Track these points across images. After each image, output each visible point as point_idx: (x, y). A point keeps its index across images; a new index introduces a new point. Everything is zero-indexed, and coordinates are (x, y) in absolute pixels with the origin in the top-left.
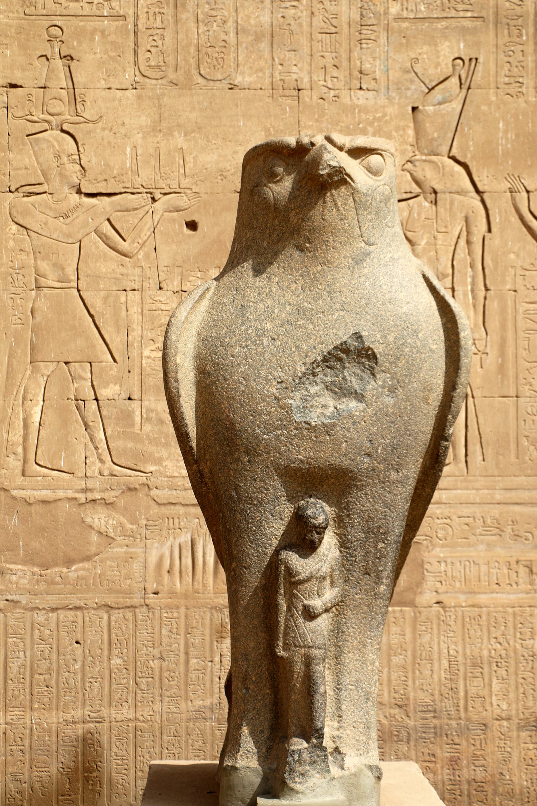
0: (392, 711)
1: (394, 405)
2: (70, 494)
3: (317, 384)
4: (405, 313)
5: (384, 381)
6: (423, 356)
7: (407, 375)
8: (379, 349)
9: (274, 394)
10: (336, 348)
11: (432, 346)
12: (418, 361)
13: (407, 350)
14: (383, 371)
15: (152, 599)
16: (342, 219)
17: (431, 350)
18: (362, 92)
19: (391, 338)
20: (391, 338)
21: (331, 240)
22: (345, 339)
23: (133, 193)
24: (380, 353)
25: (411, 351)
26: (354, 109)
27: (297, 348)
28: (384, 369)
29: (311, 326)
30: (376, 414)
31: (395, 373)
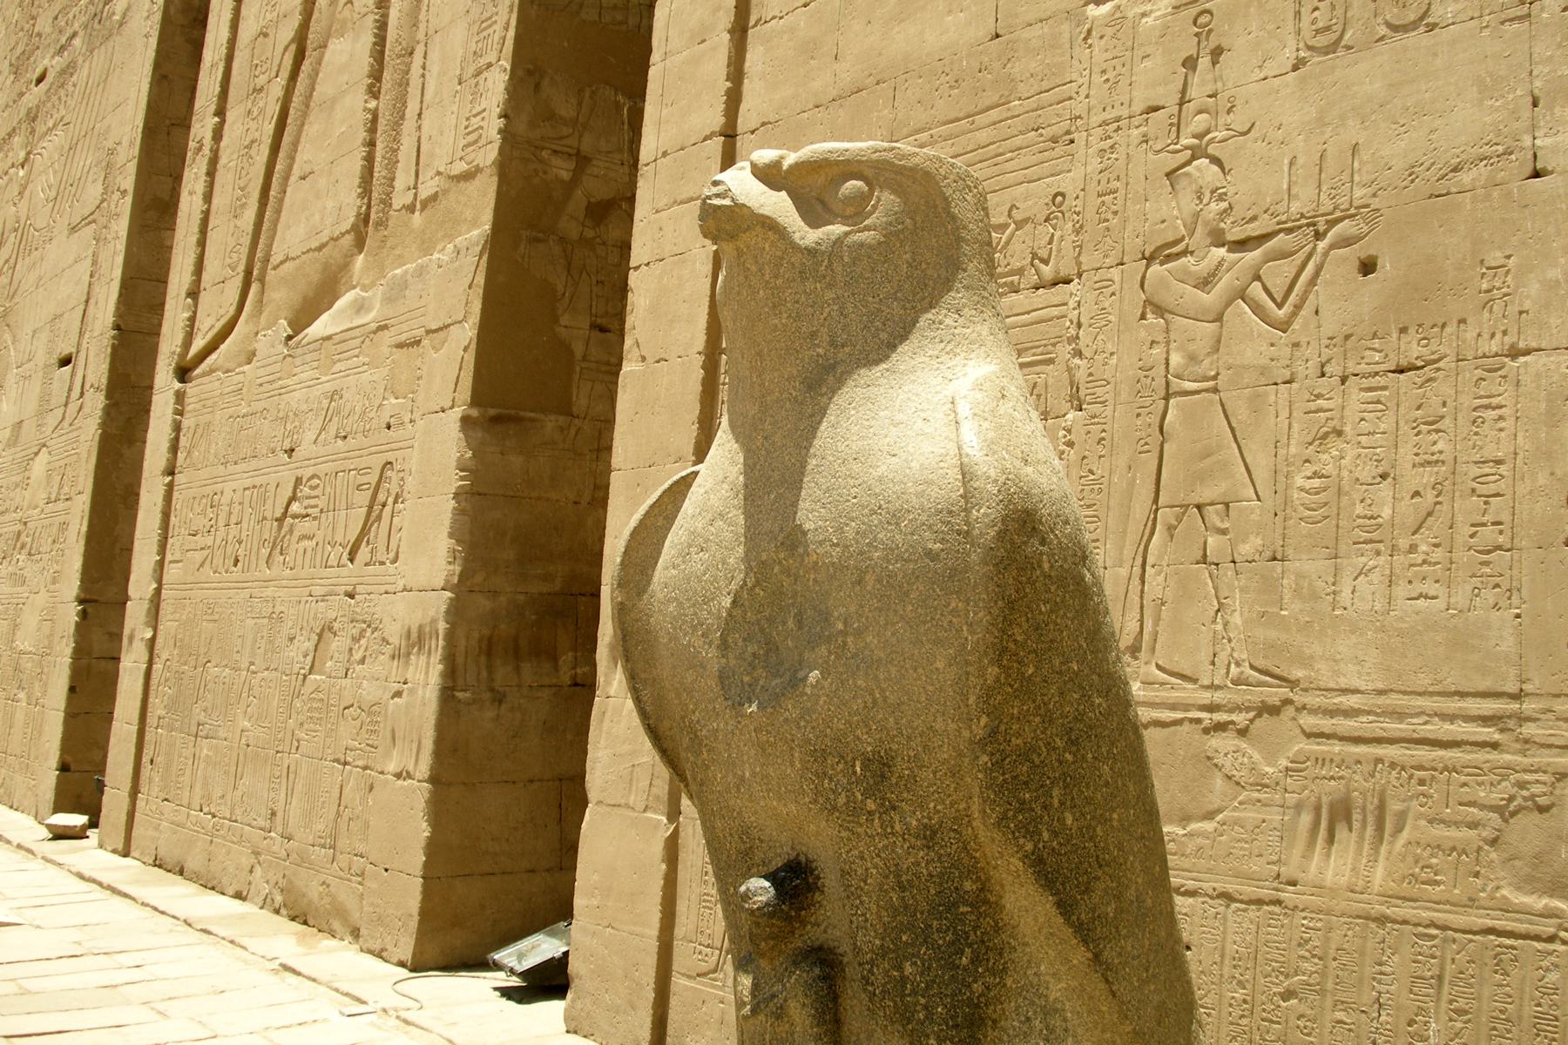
15: (1288, 895)
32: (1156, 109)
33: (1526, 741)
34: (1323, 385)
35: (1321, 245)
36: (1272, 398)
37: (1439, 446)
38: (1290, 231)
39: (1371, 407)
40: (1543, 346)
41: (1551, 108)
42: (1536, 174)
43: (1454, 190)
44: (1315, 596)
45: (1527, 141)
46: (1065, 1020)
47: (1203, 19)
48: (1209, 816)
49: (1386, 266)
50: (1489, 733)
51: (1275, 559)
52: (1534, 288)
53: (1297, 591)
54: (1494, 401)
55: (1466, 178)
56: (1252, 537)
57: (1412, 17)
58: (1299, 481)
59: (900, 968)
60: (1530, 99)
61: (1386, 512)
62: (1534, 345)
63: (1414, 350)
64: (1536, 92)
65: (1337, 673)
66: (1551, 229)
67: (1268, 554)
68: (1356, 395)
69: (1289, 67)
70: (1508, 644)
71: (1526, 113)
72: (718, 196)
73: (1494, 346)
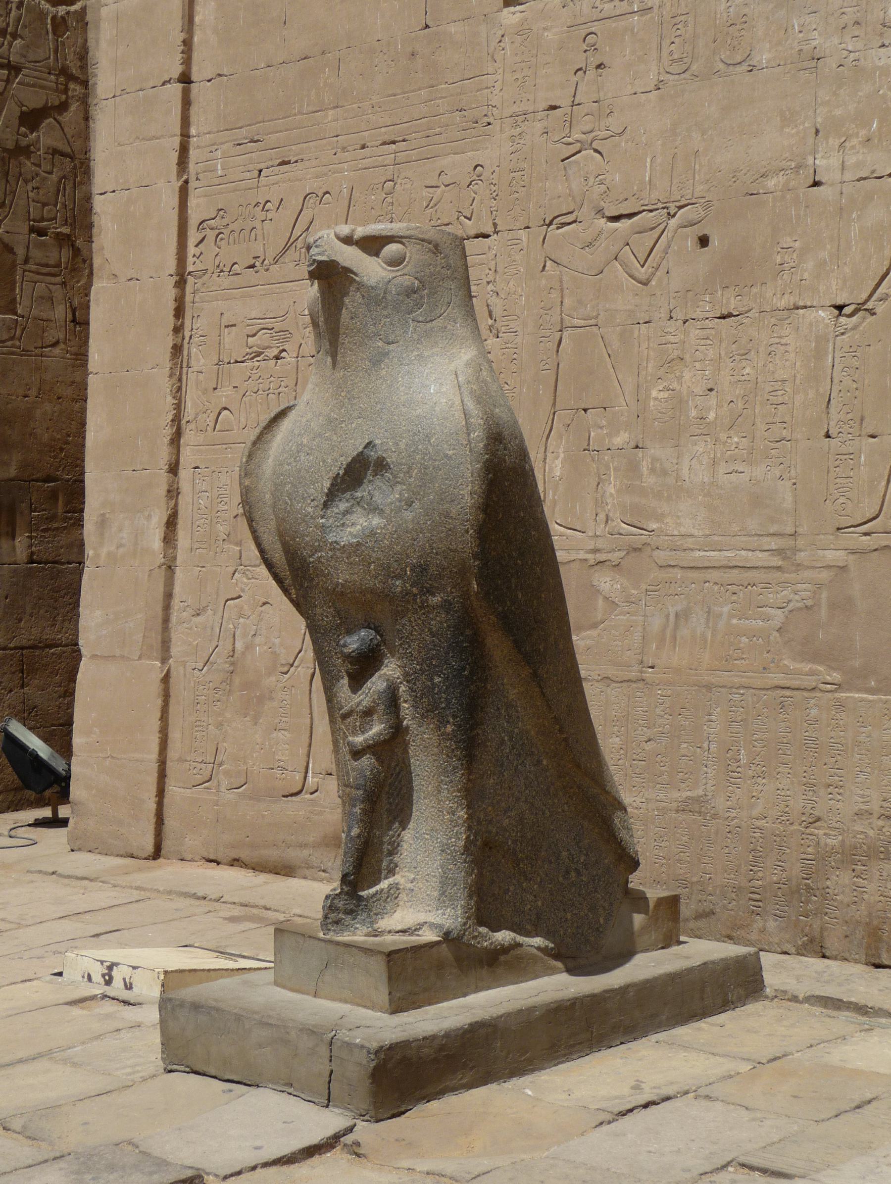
0: (881, 823)
1: (413, 521)
2: (582, 555)
4: (418, 416)
5: (400, 494)
7: (421, 486)
9: (309, 513)
17: (446, 456)
18: (883, 50)
20: (402, 446)
22: (360, 449)
24: (393, 462)
25: (423, 458)
26: (875, 73)
27: (324, 461)
29: (335, 437)
30: (396, 531)
32: (554, 108)
33: (799, 565)
34: (671, 327)
35: (673, 222)
36: (636, 333)
37: (747, 370)
38: (651, 211)
39: (703, 342)
40: (814, 304)
41: (827, 139)
42: (816, 184)
43: (761, 191)
44: (665, 473)
45: (810, 160)
46: (517, 712)
47: (591, 39)
48: (594, 626)
49: (714, 242)
50: (776, 561)
51: (637, 447)
52: (810, 265)
53: (653, 470)
54: (783, 341)
55: (771, 183)
56: (622, 433)
57: (739, 58)
58: (654, 393)
59: (432, 680)
60: (814, 131)
61: (712, 416)
62: (809, 304)
63: (733, 305)
64: (818, 126)
65: (679, 525)
66: (823, 224)
67: (633, 444)
68: (695, 332)
69: (652, 87)
70: (788, 503)
71: (811, 140)
72: (319, 254)
73: (782, 304)
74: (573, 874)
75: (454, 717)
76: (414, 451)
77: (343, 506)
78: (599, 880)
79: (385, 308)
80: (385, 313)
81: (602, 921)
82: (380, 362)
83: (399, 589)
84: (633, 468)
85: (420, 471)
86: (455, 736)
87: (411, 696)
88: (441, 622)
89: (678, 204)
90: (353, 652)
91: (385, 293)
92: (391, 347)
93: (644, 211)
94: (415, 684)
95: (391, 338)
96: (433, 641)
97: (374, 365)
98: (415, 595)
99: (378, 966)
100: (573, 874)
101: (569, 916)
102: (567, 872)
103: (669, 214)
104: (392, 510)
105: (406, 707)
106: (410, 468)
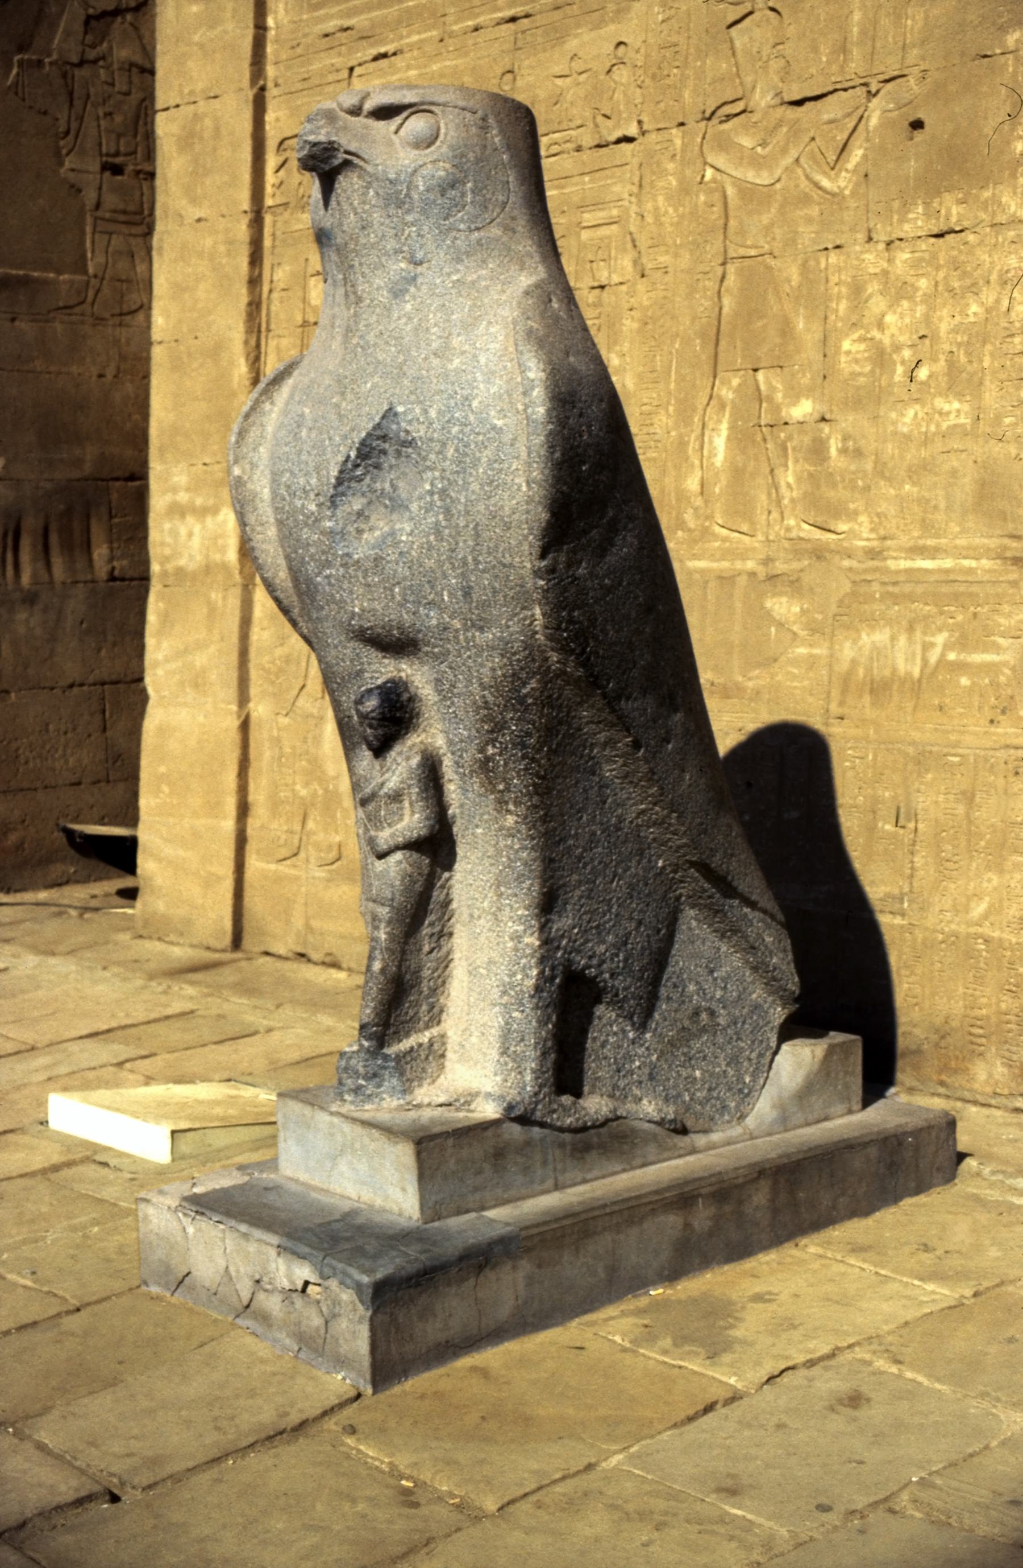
3: (363, 495)
5: (432, 485)
6: (481, 438)
7: (457, 472)
8: (419, 432)
10: (369, 435)
11: (496, 421)
12: (473, 446)
13: (455, 430)
14: (428, 468)
16: (363, 228)
17: (494, 428)
19: (433, 414)
20: (433, 414)
21: (356, 264)
23: (845, 90)
25: (461, 431)
28: (428, 463)
31: (444, 470)
44: (859, 453)
51: (823, 419)
53: (843, 451)
58: (846, 345)
67: (817, 416)
74: (704, 1016)
75: (517, 804)
76: (448, 421)
77: (357, 504)
78: (744, 1023)
79: (408, 212)
80: (409, 218)
81: (747, 1080)
82: (404, 291)
83: (434, 622)
84: (818, 451)
85: (457, 450)
86: (519, 831)
87: (456, 772)
88: (493, 669)
89: (882, 77)
90: (372, 711)
91: (408, 188)
92: (419, 269)
93: (836, 90)
94: (461, 756)
95: (419, 255)
96: (484, 696)
97: (396, 296)
98: (457, 631)
99: (404, 1153)
100: (704, 1016)
101: (698, 1073)
102: (696, 1013)
103: (869, 92)
104: (420, 508)
105: (452, 791)
106: (444, 445)
